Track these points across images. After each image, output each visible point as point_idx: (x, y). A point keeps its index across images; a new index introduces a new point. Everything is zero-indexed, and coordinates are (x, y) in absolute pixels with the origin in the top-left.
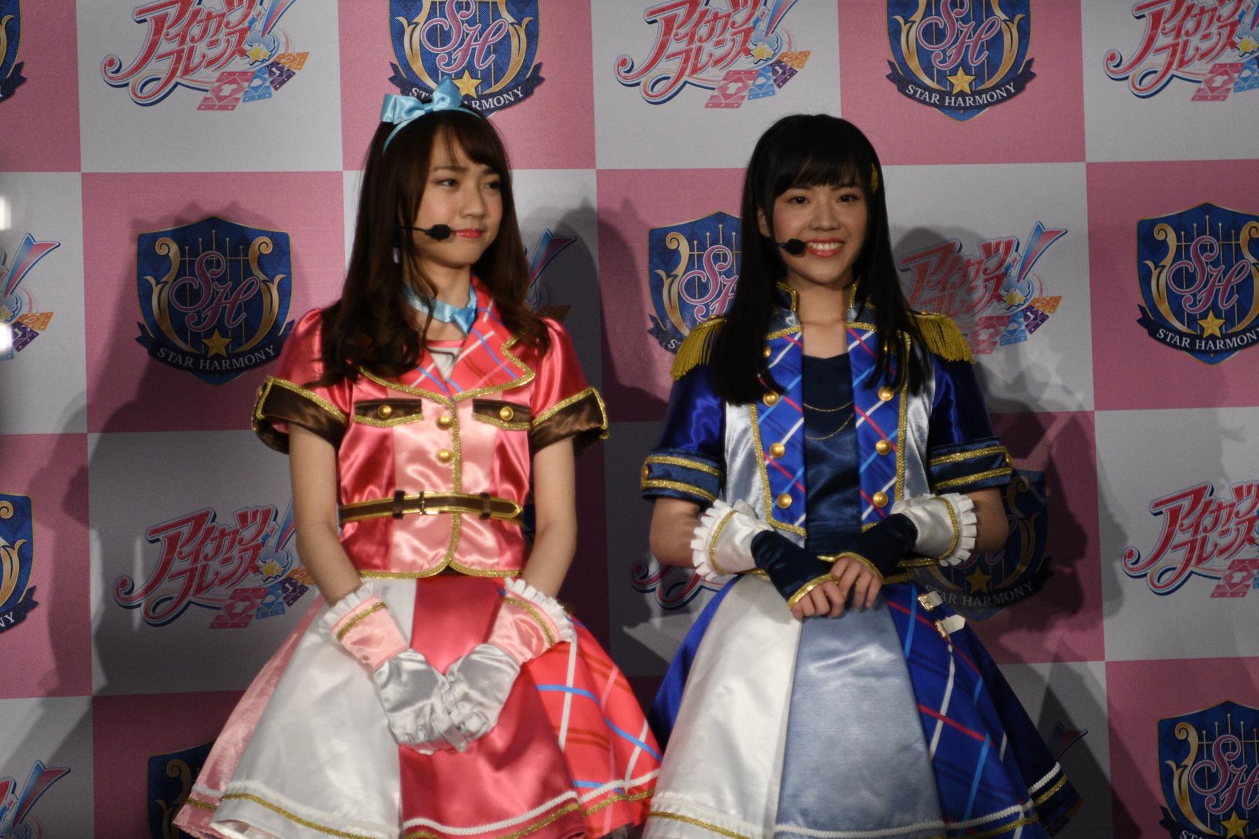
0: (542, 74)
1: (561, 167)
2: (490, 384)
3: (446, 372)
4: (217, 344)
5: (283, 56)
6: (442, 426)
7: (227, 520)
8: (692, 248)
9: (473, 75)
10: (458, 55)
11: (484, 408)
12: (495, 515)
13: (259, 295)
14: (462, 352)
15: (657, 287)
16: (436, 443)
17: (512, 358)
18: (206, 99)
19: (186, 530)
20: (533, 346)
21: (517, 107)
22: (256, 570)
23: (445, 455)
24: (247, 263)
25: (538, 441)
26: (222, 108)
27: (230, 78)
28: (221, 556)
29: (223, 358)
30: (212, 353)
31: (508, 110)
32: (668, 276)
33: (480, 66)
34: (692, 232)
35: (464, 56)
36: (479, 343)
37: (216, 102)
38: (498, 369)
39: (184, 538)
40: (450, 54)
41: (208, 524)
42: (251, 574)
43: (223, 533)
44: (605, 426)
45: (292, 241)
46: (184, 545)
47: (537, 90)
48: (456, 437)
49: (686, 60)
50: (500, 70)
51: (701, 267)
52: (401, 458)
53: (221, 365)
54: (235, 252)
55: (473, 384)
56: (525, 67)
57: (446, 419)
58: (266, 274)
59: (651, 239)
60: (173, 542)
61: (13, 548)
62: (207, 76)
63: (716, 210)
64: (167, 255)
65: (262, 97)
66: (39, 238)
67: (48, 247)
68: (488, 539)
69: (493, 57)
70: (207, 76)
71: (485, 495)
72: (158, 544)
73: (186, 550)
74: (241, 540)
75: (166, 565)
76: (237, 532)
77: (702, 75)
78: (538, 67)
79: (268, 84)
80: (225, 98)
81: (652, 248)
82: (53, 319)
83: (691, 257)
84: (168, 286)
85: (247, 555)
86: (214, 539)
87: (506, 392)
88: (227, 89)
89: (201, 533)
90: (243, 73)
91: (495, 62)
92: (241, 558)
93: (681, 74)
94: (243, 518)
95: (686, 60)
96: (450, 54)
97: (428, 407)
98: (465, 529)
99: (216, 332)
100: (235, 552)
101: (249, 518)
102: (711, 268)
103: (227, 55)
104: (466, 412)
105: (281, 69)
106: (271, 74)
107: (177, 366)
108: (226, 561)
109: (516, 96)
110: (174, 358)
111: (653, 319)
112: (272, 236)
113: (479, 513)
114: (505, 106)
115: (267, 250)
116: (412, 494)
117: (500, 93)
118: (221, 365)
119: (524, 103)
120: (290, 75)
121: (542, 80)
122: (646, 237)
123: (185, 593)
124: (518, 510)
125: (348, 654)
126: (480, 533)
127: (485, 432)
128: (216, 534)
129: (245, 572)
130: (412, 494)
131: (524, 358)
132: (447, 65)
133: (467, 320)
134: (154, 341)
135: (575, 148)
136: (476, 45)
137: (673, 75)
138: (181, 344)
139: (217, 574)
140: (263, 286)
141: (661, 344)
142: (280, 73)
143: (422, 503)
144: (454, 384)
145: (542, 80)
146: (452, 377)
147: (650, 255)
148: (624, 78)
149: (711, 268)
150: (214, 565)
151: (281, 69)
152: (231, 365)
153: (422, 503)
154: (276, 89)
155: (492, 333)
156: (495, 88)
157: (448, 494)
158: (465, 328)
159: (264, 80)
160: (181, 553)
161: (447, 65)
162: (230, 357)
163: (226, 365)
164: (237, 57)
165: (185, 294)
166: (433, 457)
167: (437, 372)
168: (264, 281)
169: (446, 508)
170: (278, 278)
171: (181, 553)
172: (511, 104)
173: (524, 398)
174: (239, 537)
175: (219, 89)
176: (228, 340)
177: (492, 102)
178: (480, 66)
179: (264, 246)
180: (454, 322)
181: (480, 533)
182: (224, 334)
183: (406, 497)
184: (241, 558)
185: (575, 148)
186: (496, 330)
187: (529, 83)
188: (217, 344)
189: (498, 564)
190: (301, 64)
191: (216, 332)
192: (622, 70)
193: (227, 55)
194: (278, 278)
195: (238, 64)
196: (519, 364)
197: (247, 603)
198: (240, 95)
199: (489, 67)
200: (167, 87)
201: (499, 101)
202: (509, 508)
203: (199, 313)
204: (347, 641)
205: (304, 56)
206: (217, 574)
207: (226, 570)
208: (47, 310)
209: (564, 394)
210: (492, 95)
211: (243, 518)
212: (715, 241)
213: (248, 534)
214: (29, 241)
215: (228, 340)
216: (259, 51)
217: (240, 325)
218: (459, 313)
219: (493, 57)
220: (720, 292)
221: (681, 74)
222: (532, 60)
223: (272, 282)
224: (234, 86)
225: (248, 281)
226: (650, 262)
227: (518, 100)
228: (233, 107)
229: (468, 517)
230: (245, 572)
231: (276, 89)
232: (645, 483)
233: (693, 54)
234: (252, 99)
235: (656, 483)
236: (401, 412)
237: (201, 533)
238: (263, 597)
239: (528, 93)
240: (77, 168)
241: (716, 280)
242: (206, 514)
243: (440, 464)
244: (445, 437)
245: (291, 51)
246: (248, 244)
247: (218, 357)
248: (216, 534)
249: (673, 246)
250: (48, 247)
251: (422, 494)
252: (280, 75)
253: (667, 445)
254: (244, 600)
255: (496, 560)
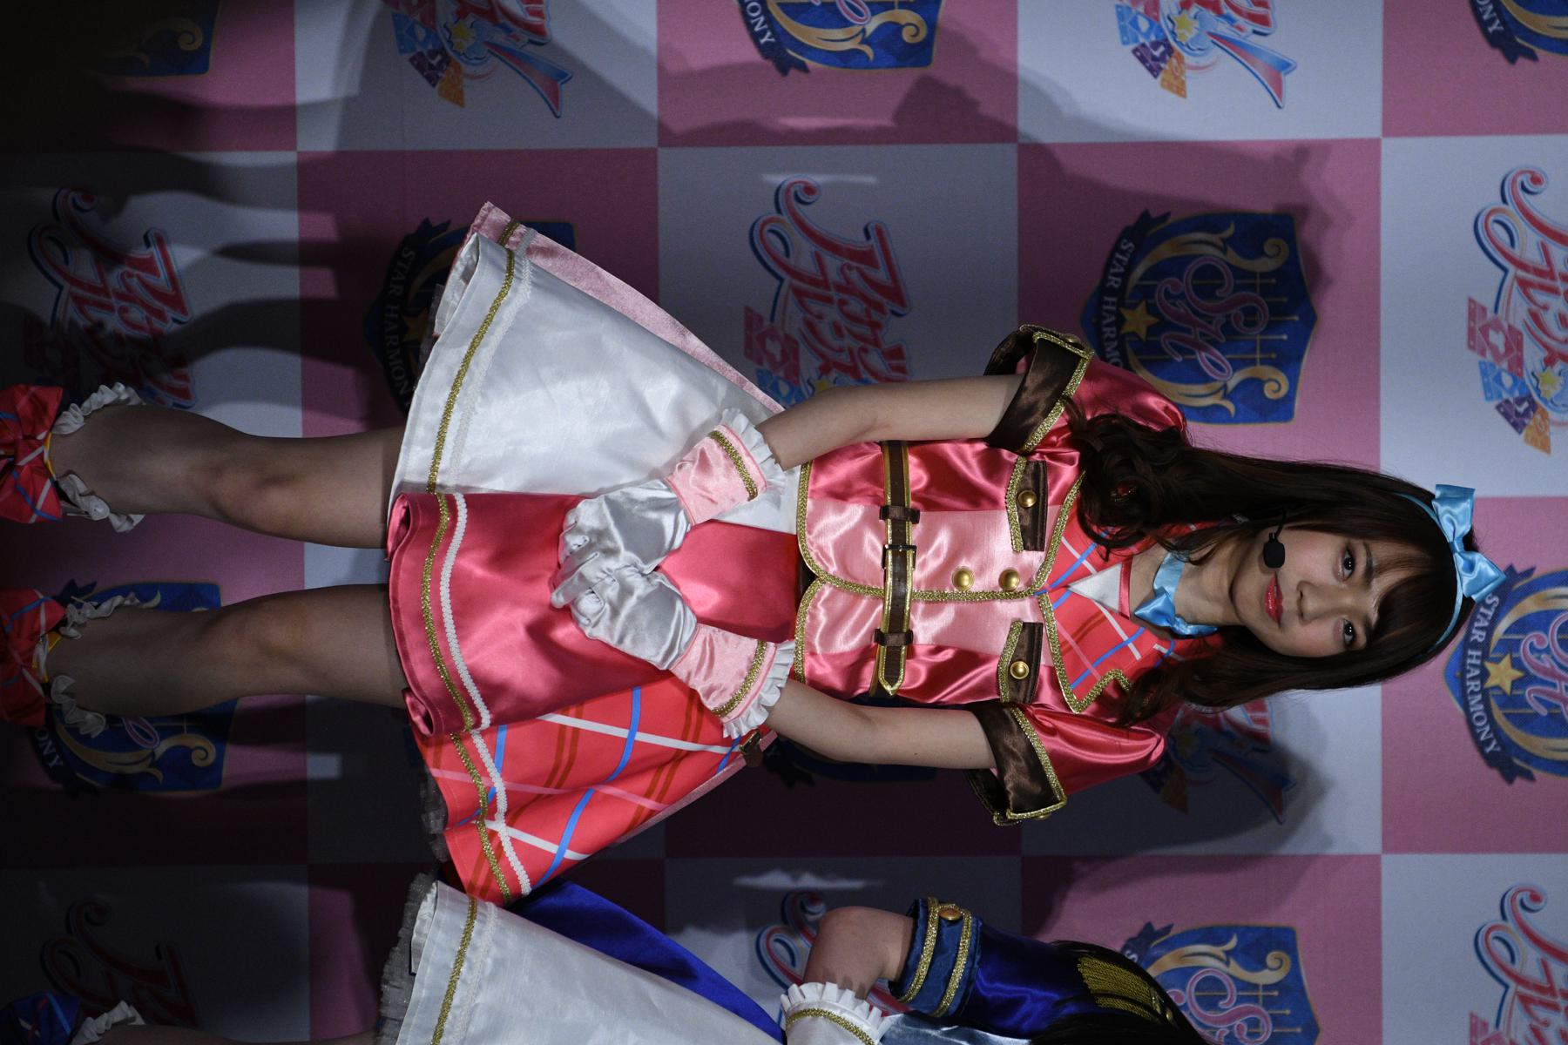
0: (1518, 782)
1: (1385, 806)
2: (1065, 649)
3: (1087, 588)
4: (1138, 321)
5: (1545, 416)
6: (1006, 576)
7: (893, 332)
8: (1267, 987)
9: (1516, 684)
10: (1547, 662)
11: (1031, 636)
12: (882, 649)
13: (1205, 379)
14: (1111, 612)
15: (1212, 935)
16: (982, 570)
17: (1104, 681)
18: (1484, 310)
19: (881, 275)
20: (1119, 710)
21: (1470, 743)
22: (824, 370)
23: (966, 580)
24: (1253, 362)
25: (991, 714)
26: (1471, 332)
27: (1514, 341)
28: (844, 323)
29: (1119, 329)
30: (1127, 314)
31: (1465, 732)
32: (1228, 953)
33: (1529, 693)
34: (1291, 989)
35: (1545, 671)
36: (1125, 638)
37: (1479, 324)
38: (1086, 662)
39: (870, 272)
40: (1547, 650)
41: (889, 305)
42: (818, 363)
43: (875, 326)
44: (1011, 815)
45: (1282, 425)
46: (862, 274)
47: (1494, 774)
48: (991, 596)
49: (1538, 988)
50: (1526, 721)
51: (1240, 1000)
52: (965, 518)
53: (1108, 325)
54: (1267, 347)
55: (1064, 624)
56: (1529, 757)
57: (1015, 582)
58: (1237, 387)
59: (1280, 930)
60: (865, 257)
61: (862, 42)
62: (1517, 312)
63: (1321, 1023)
64: (1263, 254)
65: (1487, 387)
66: (1288, 80)
67: (1276, 89)
68: (847, 643)
69: (1543, 712)
70: (1517, 312)
71: (910, 637)
72: (862, 237)
73: (854, 276)
74: (866, 351)
75: (833, 248)
76: (876, 343)
77: (1518, 1011)
78: (1529, 776)
79: (1505, 396)
80: (1486, 335)
81: (1268, 931)
82: (1173, 97)
83: (1255, 987)
84: (1221, 255)
85: (844, 358)
86: (868, 314)
87: (1052, 670)
88: (1498, 339)
89: (876, 296)
90: (1520, 362)
91: (1536, 715)
92: (841, 350)
93: (1519, 980)
94: (896, 353)
95: (1538, 988)
96: (1547, 650)
97: (1033, 558)
98: (864, 602)
99: (1152, 320)
100: (849, 342)
101: (894, 362)
102: (1240, 1014)
103: (1546, 339)
104: (1024, 610)
105: (1526, 414)
106: (1519, 401)
107: (1109, 265)
108: (837, 329)
109: (1488, 742)
110: (1120, 261)
111: (1168, 929)
112: (1289, 399)
113: (883, 628)
114: (1472, 728)
115: (1269, 391)
116: (914, 533)
117: (1491, 721)
118: (1108, 325)
119: (1477, 754)
120: (1518, 427)
121: (1510, 780)
122: (1283, 923)
123: (797, 275)
124: (888, 688)
125: (690, 443)
126: (855, 630)
127: (999, 641)
128: (875, 316)
129: (822, 355)
130: (914, 533)
131: (1102, 699)
132: (1532, 647)
133: (1157, 613)
134: (1147, 228)
135: (1413, 822)
136: (1560, 688)
137: (1517, 968)
138: (1139, 270)
139: (820, 317)
140: (1219, 385)
141: (1131, 940)
142: (1520, 413)
143: (900, 551)
144: (1065, 596)
145: (1510, 780)
146: (1074, 594)
147: (1258, 928)
148: (1513, 899)
149: (1240, 1014)
150: (832, 313)
151: (1526, 414)
152: (1109, 339)
153: (900, 551)
154: (1498, 407)
155: (1138, 656)
156: (1498, 714)
157: (909, 585)
158: (1146, 611)
159: (1511, 391)
160: (850, 268)
161: (1532, 647)
162: (1121, 338)
163: (1109, 332)
164: (1543, 354)
165: (1208, 278)
166: (963, 563)
167: (1086, 574)
168: (1225, 386)
169: (890, 580)
170: (1230, 406)
171: (850, 268)
172: (1475, 735)
173: (1046, 696)
174: (870, 347)
175: (1497, 326)
176: (1143, 336)
177: (1478, 709)
178: (1529, 693)
179: (1275, 385)
180: (1156, 594)
181: (855, 630)
182: (1151, 330)
183: (909, 524)
184: (841, 350)
185: (1413, 822)
186: (1144, 659)
187: (1506, 762)
188: (1138, 321)
189: (813, 654)
190: (1533, 442)
191: (1152, 320)
192: (1525, 896)
193: (1546, 339)
194: (1230, 406)
195: (1533, 356)
196: (1095, 692)
197: (778, 358)
198: (1489, 357)
199: (1527, 705)
200: (1502, 257)
201: (1479, 719)
202: (892, 677)
203: (1182, 296)
204: (708, 444)
205: (1545, 447)
206: (820, 317)
207: (825, 328)
208: (1189, 94)
209: (1055, 757)
210: (1488, 709)
211: (896, 353)
212: (1277, 1021)
213: (875, 360)
214: (1286, 66)
215: (1143, 336)
216: (1553, 384)
217: (1164, 353)
218: (1167, 601)
219: (1543, 712)
220: (1206, 1027)
221: (1519, 980)
222: (1538, 767)
223: (1226, 397)
224: (1502, 349)
225: (1227, 366)
226: (1248, 928)
227: (1481, 746)
228: (1472, 347)
229: (878, 615)
230: (822, 355)
231: (1498, 407)
232: (935, 911)
233: (1547, 998)
234: (1484, 373)
235: (933, 931)
236: (1027, 522)
237: (876, 296)
238: (787, 379)
239: (1492, 760)
240: (1388, 131)
241: (1221, 1021)
242: (902, 303)
243: (953, 572)
244: (992, 579)
245: (1552, 428)
246: (1277, 364)
247: (1120, 322)
248: (875, 316)
249: (1271, 959)
250: (1276, 89)
251: (914, 548)
252: (1517, 414)
253: (987, 944)
254: (783, 352)
255: (818, 650)
